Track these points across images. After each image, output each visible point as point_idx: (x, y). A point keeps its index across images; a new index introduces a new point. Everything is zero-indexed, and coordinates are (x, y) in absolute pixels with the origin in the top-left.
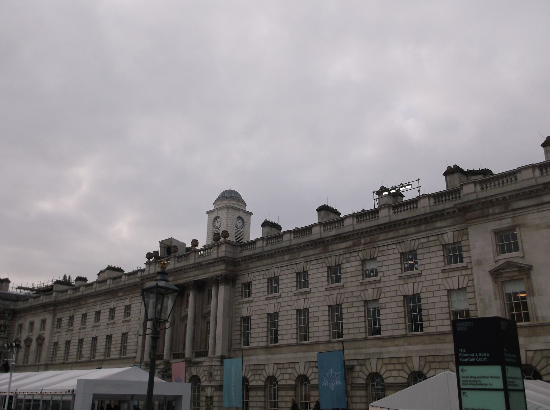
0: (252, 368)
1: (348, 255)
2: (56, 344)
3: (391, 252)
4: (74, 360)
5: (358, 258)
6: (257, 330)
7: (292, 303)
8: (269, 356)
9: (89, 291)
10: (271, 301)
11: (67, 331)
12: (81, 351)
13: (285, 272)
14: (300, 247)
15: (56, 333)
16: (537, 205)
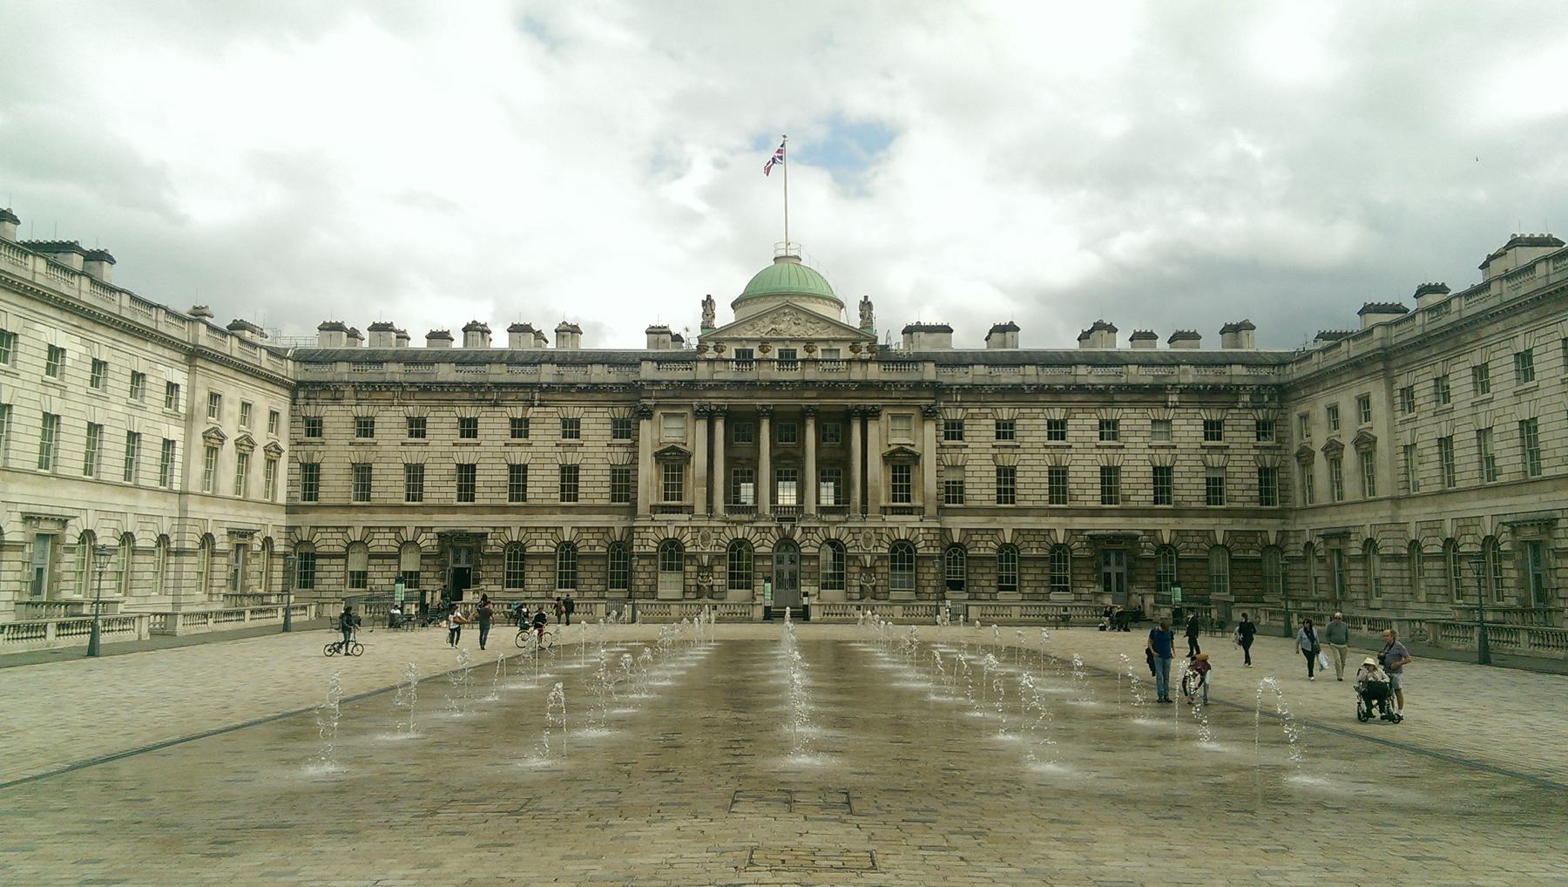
2: (1409, 449)
4: (1477, 483)
9: (1479, 309)
11: (1435, 414)
15: (1402, 423)
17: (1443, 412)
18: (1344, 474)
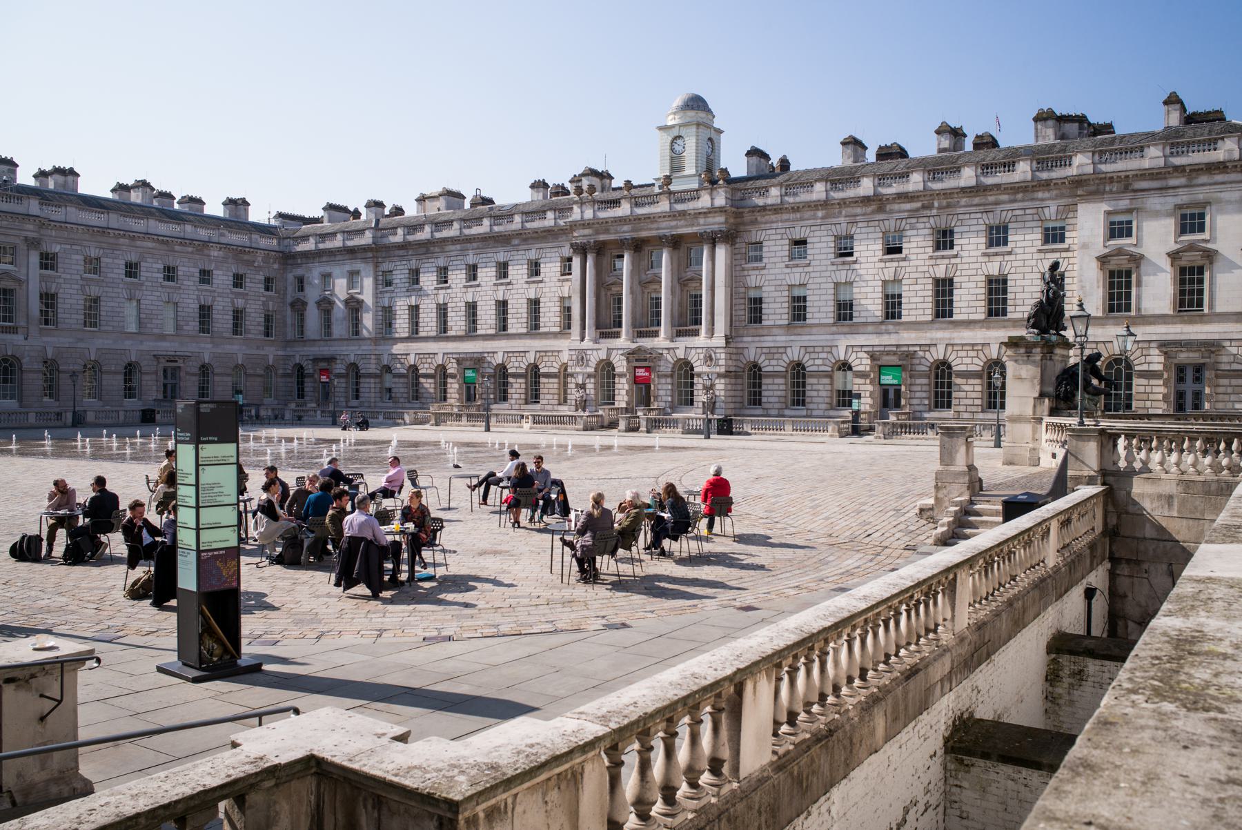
1: (914, 220)
3: (974, 222)
5: (928, 225)
7: (828, 274)
8: (793, 338)
10: (795, 270)
12: (445, 322)
13: (817, 234)
16: (1161, 189)
17: (414, 290)
18: (333, 320)
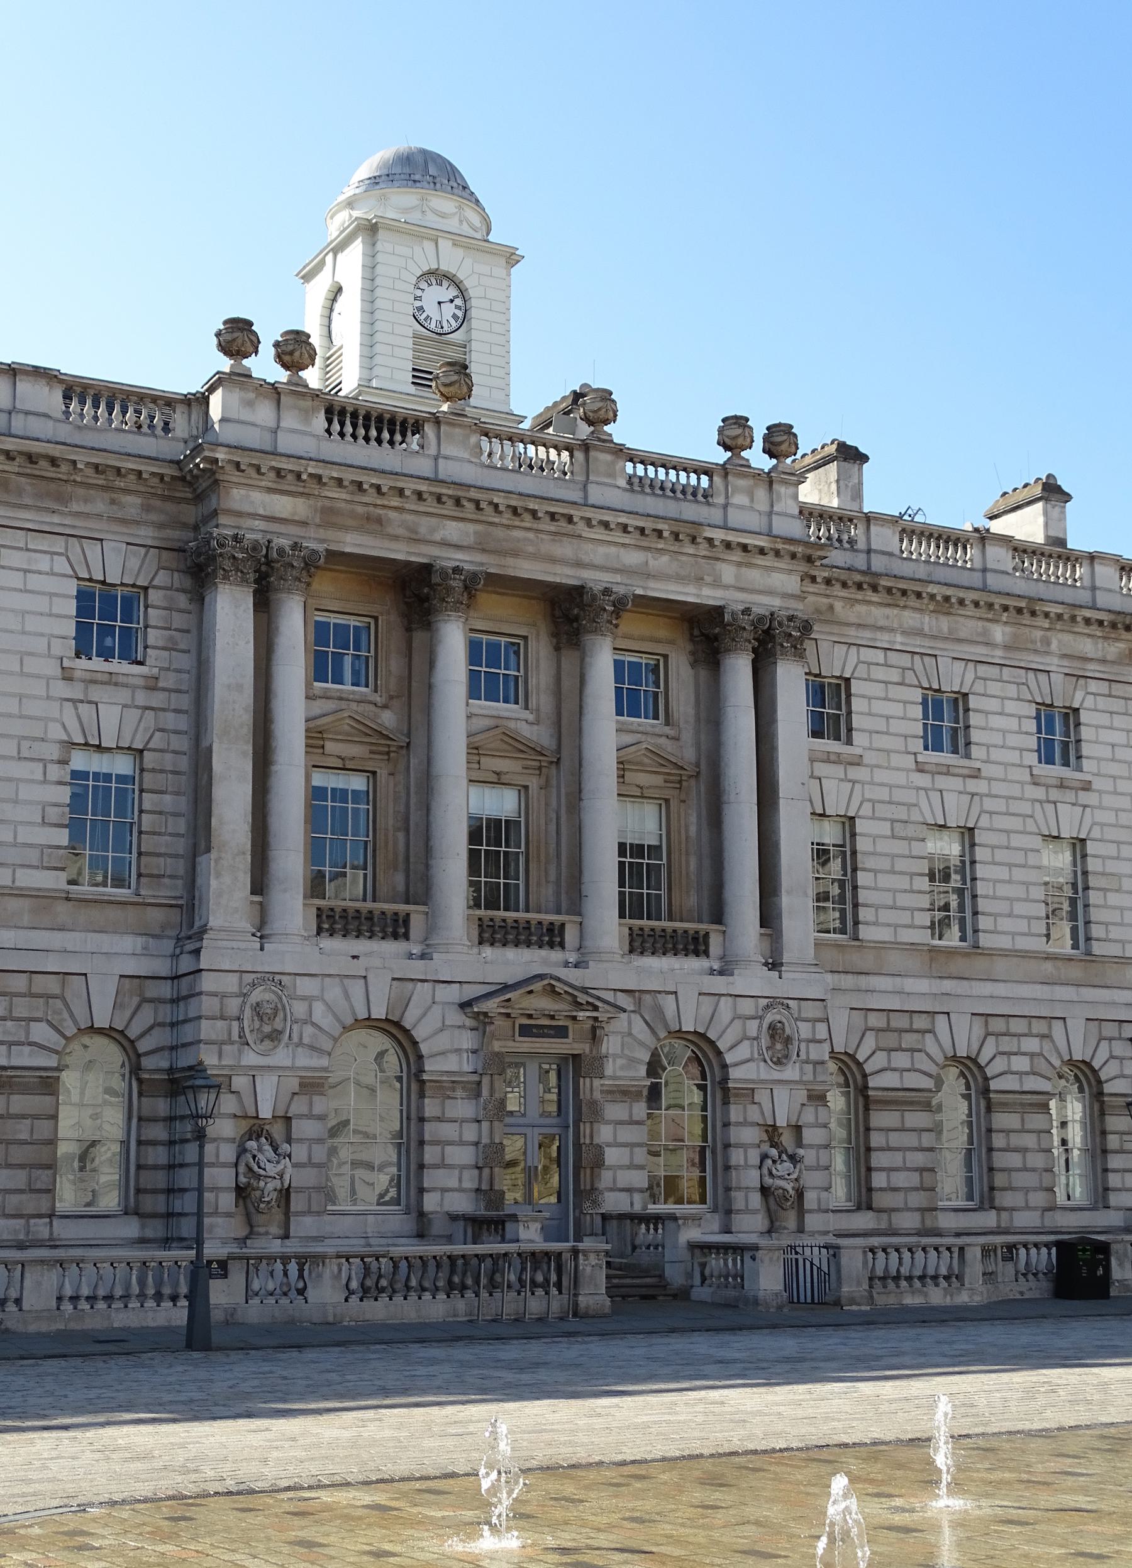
0: (875, 1020)
6: (884, 881)
8: (948, 985)
14: (1073, 618)
